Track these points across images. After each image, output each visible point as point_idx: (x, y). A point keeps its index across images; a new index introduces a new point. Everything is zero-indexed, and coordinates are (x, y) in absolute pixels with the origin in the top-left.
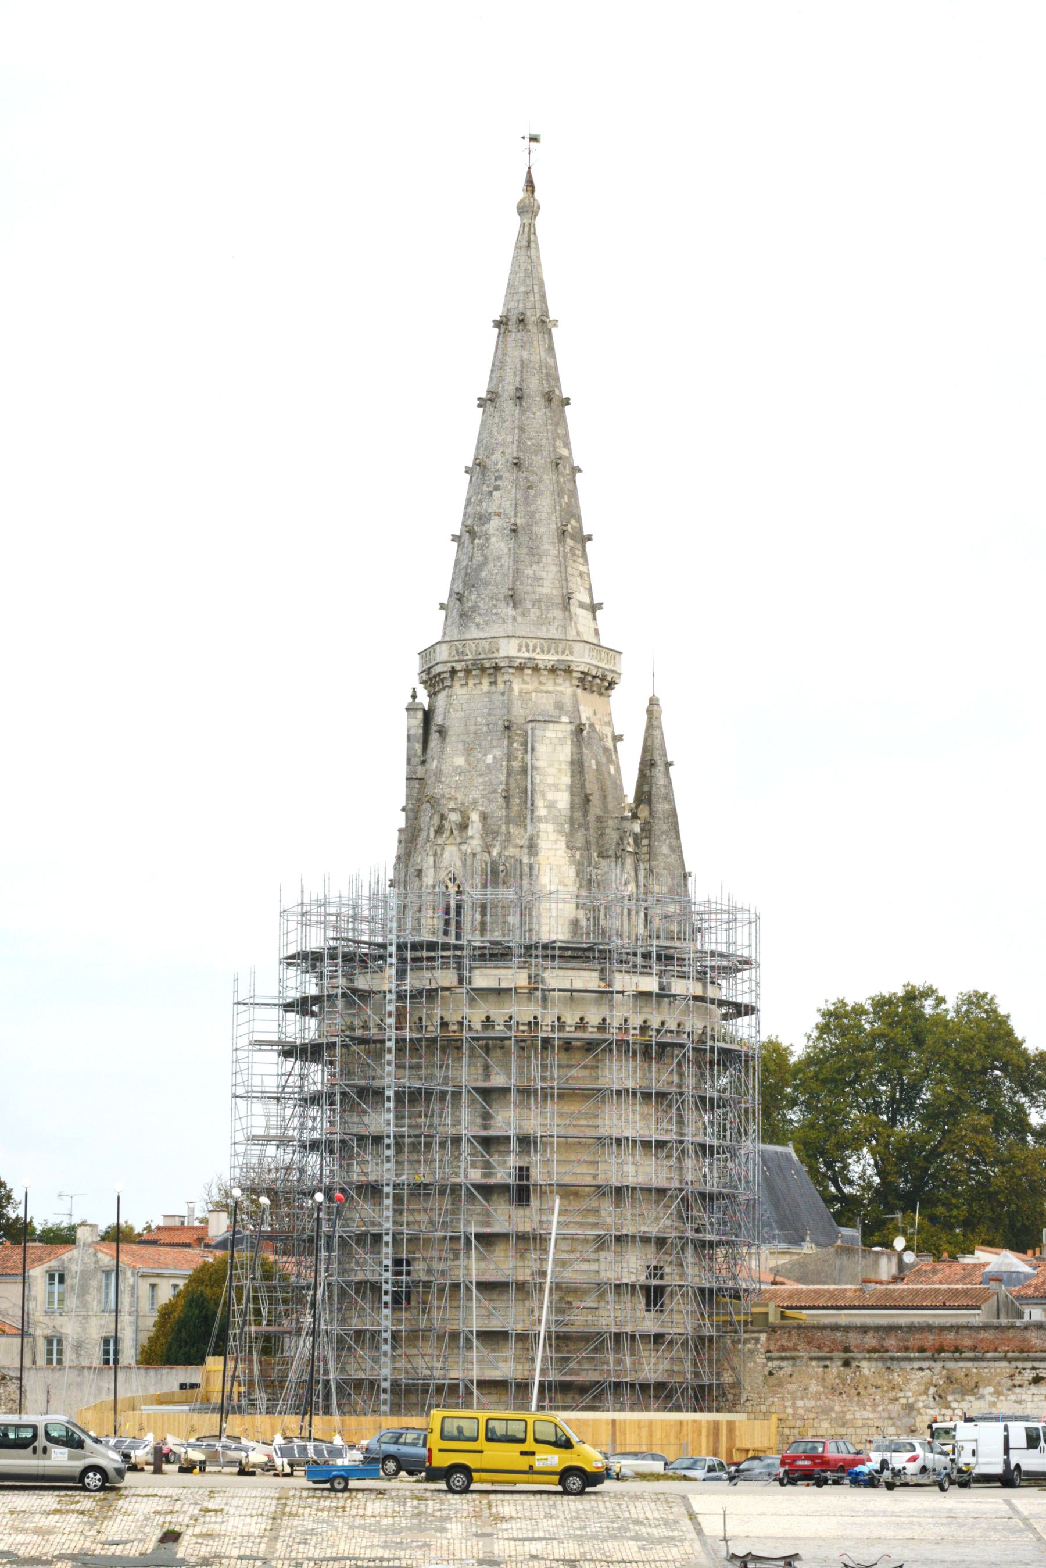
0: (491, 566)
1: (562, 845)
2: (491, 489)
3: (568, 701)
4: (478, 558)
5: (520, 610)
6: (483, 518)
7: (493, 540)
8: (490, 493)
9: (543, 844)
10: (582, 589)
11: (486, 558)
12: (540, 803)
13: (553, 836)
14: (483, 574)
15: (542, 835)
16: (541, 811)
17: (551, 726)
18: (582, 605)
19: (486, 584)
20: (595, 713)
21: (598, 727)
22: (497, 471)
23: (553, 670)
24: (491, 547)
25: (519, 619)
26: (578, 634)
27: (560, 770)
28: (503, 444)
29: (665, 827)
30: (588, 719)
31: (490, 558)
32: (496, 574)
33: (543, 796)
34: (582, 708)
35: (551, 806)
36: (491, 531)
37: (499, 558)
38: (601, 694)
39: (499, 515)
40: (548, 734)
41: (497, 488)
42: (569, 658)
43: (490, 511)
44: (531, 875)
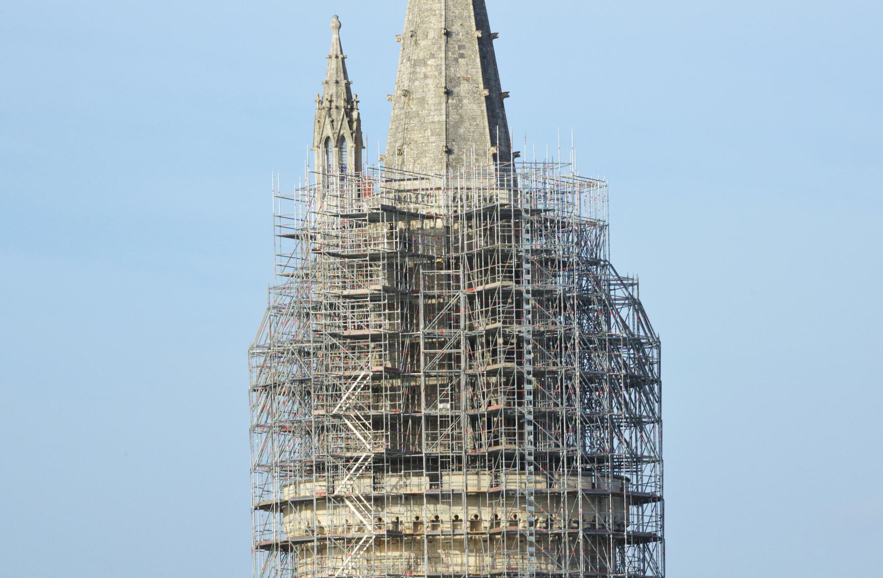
0: (467, 124)
2: (456, 56)
4: (454, 117)
6: (457, 81)
7: (465, 101)
8: (456, 60)
11: (462, 118)
14: (462, 131)
19: (465, 140)
22: (459, 40)
24: (465, 108)
28: (461, 18)
31: (465, 118)
32: (473, 132)
36: (462, 94)
37: (474, 119)
39: (467, 80)
41: (462, 56)
43: (458, 75)
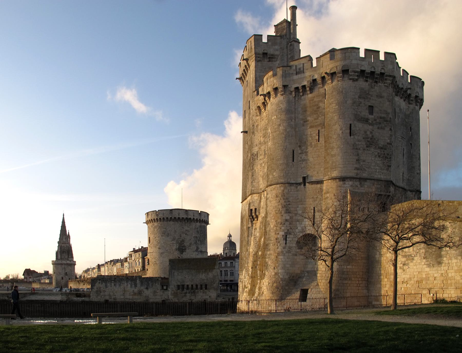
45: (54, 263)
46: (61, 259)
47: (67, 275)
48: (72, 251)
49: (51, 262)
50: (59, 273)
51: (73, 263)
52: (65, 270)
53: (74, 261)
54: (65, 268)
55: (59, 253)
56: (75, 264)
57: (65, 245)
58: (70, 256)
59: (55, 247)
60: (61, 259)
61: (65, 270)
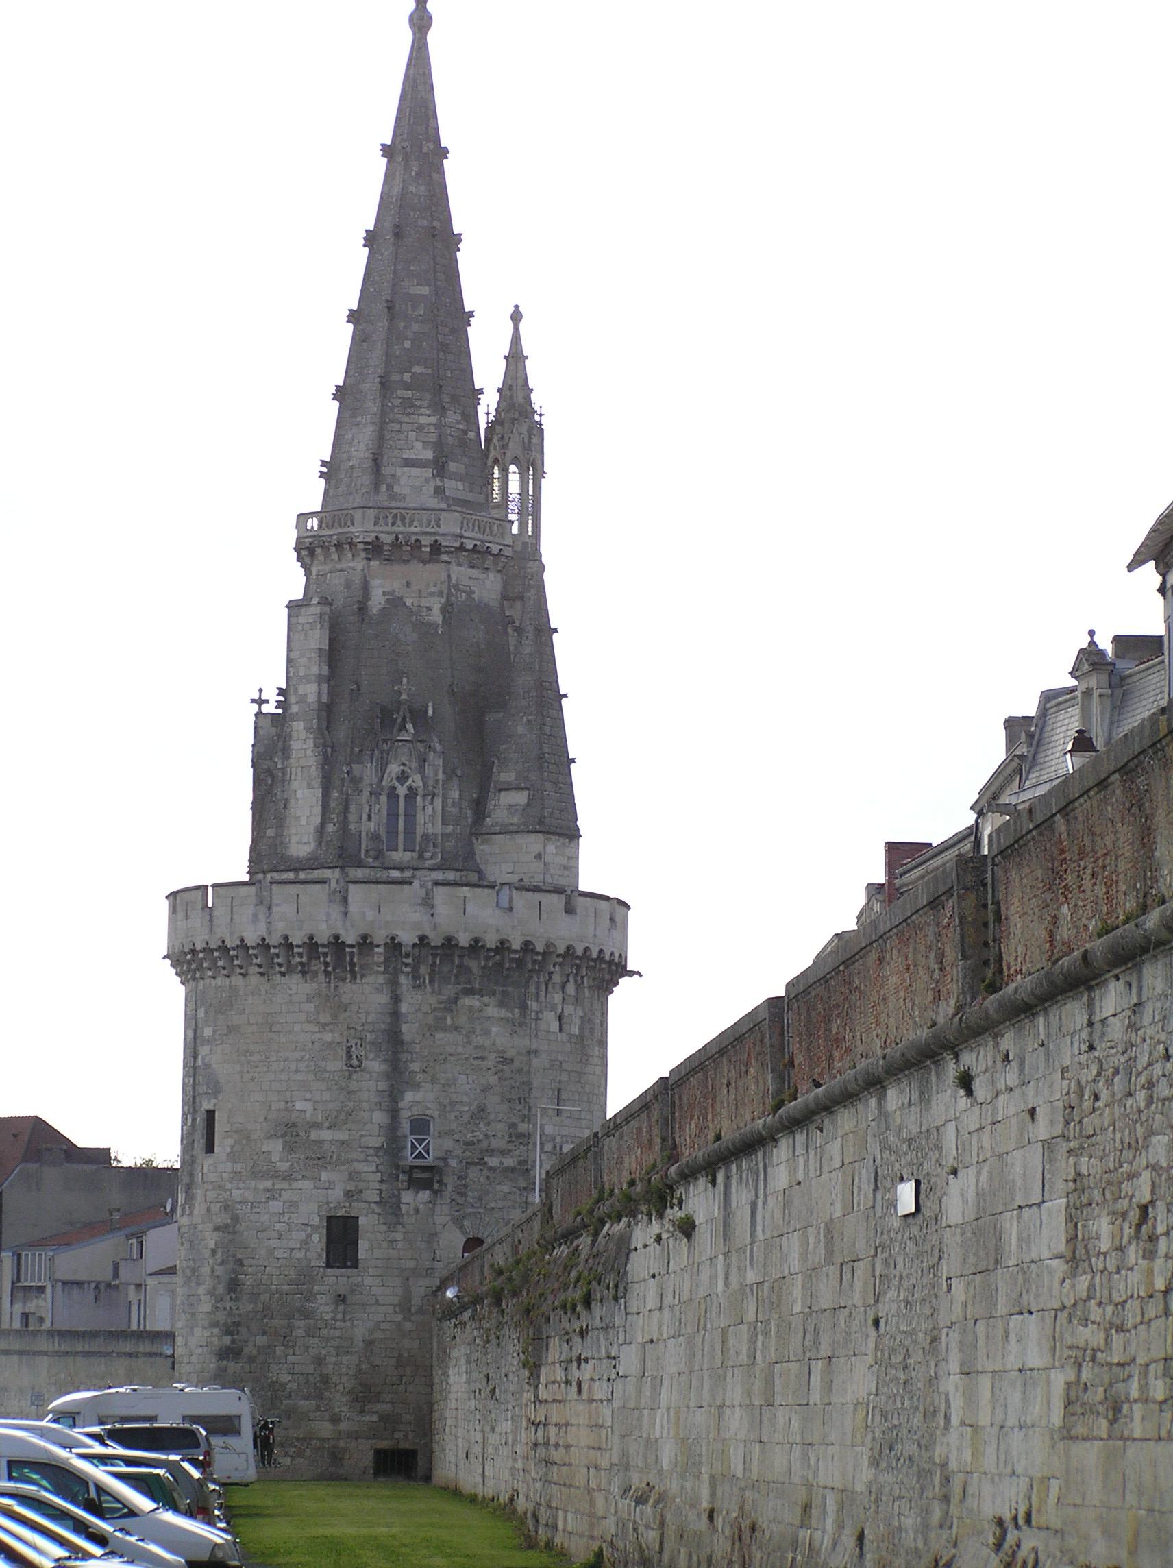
1: (311, 743)
3: (357, 579)
5: (333, 482)
9: (295, 745)
10: (419, 445)
12: (293, 699)
13: (303, 735)
15: (294, 734)
16: (294, 709)
17: (303, 610)
18: (409, 463)
20: (408, 585)
21: (409, 602)
23: (339, 546)
25: (331, 492)
26: (393, 497)
27: (310, 658)
29: (524, 703)
30: (384, 594)
33: (296, 691)
34: (375, 583)
35: (302, 700)
38: (424, 562)
40: (302, 620)
42: (352, 529)
44: (283, 781)
45: (211, 948)
46: (344, 854)
47: (426, 1177)
48: (548, 698)
49: (154, 931)
50: (290, 1132)
51: (562, 931)
52: (398, 1078)
53: (571, 898)
54: (394, 1042)
55: (303, 746)
56: (609, 969)
57: (421, 589)
58: (507, 804)
59: (239, 638)
60: (344, 854)
61: (398, 1078)
